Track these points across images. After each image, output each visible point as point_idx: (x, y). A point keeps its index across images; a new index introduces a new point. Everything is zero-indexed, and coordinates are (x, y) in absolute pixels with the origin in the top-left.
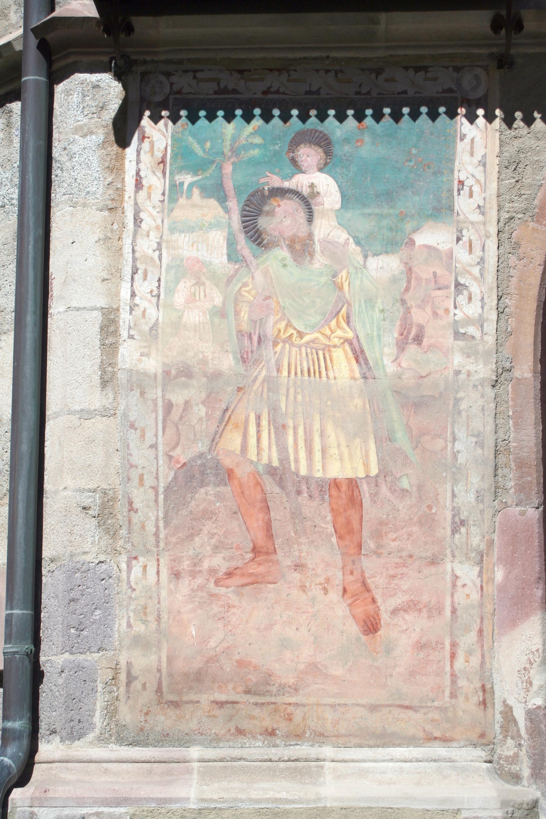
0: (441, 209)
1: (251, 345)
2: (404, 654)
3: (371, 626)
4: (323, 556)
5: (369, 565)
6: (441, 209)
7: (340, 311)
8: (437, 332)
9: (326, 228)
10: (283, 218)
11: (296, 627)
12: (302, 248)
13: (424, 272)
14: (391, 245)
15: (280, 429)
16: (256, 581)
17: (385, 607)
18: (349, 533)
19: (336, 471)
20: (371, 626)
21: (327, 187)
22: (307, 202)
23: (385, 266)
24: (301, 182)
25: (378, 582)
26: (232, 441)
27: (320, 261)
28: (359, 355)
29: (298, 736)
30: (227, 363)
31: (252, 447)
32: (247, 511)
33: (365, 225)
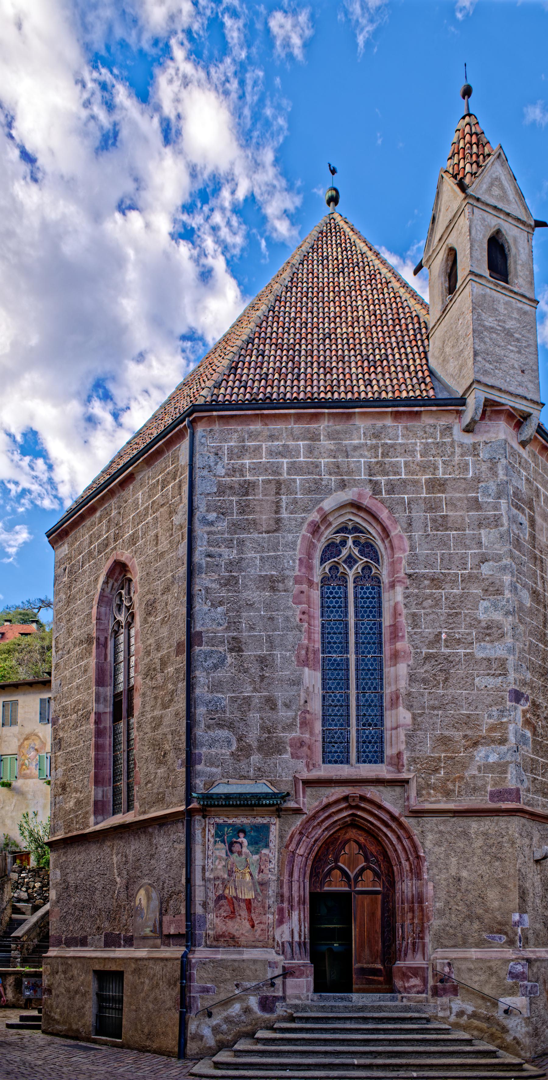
0: (267, 846)
1: (231, 873)
2: (259, 932)
3: (253, 926)
4: (244, 913)
5: (253, 915)
6: (267, 846)
7: (247, 866)
8: (266, 871)
9: (245, 850)
10: (236, 848)
11: (239, 927)
12: (240, 853)
13: (263, 858)
14: (257, 853)
15: (236, 889)
16: (232, 918)
17: (256, 923)
18: (249, 909)
19: (247, 897)
20: (253, 926)
21: (245, 842)
22: (241, 844)
23: (256, 857)
24: (240, 840)
25: (254, 918)
26: (227, 891)
27: (244, 856)
28: (251, 875)
29: (239, 946)
30: (226, 876)
31: (230, 892)
32: (230, 905)
33: (252, 849)
